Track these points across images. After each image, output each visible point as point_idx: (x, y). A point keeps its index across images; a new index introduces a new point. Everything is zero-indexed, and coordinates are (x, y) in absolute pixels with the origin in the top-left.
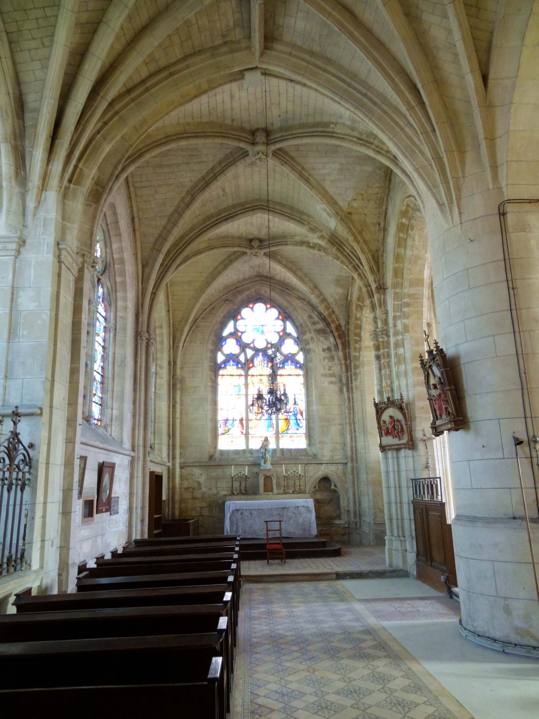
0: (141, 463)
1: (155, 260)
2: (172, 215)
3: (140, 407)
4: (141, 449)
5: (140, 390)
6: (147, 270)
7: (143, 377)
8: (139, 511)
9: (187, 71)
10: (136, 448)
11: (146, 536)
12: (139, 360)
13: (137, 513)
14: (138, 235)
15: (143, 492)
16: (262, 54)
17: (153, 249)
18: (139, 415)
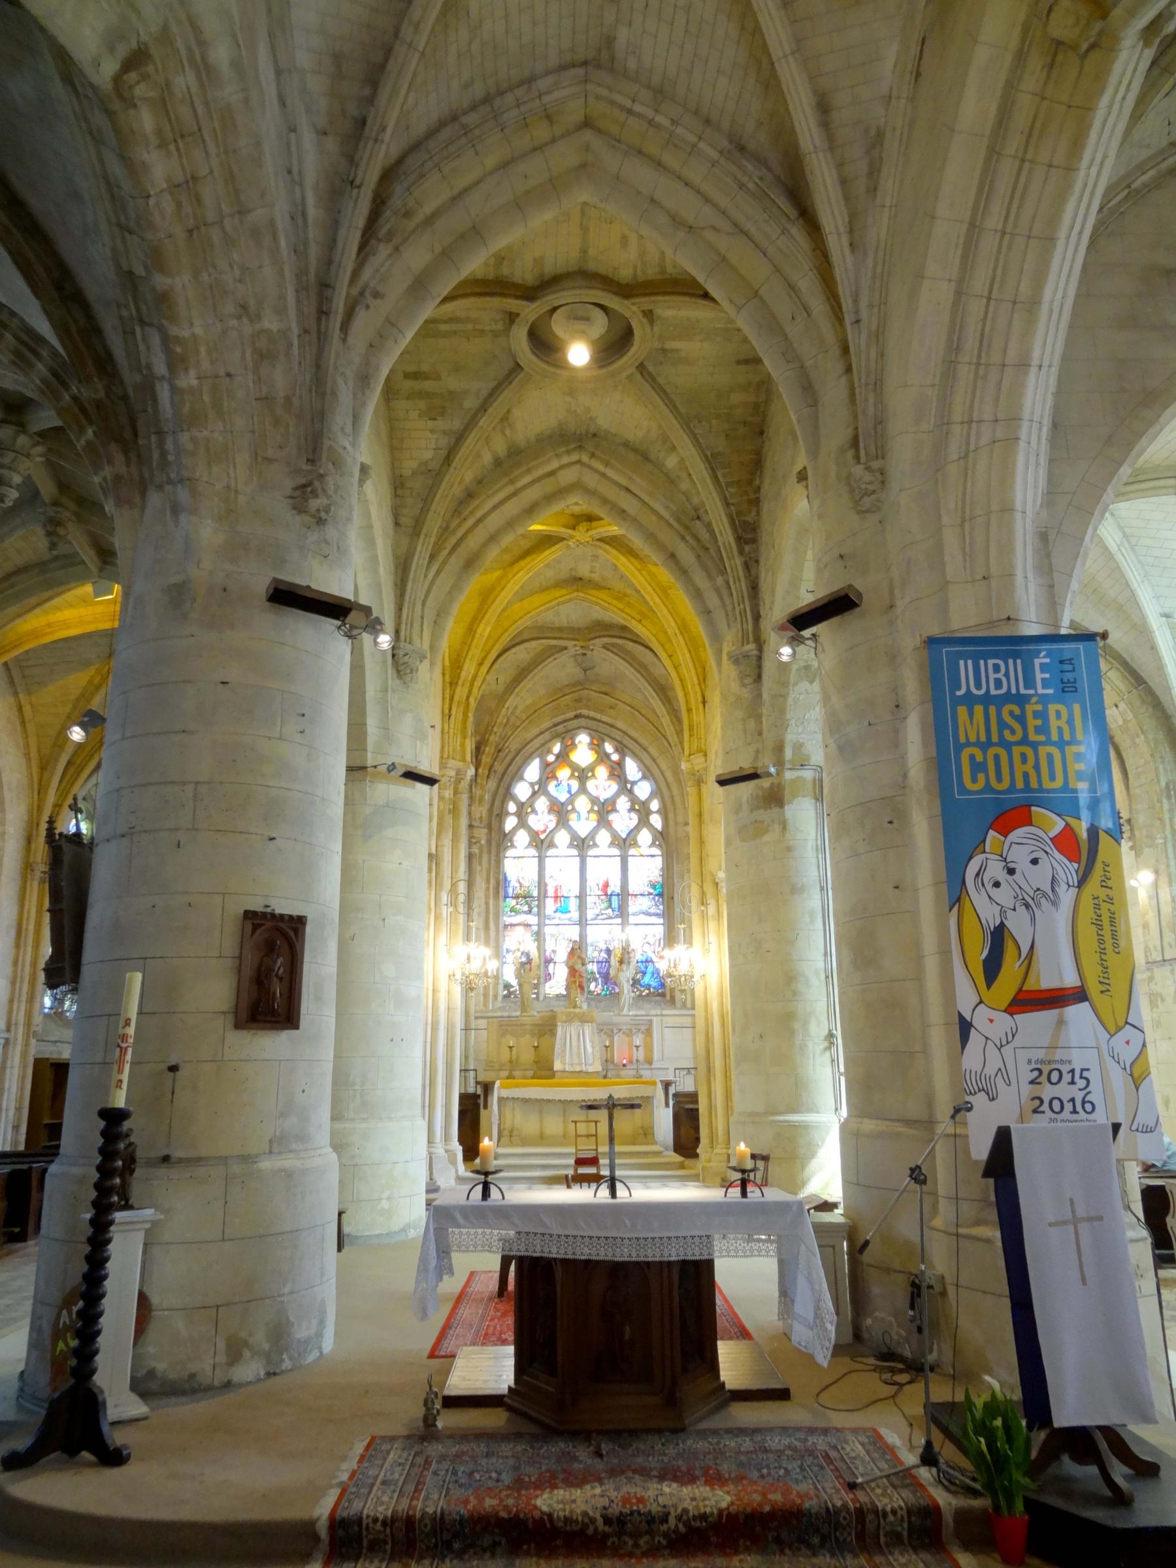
0: (19, 1048)
1: (57, 761)
2: (78, 699)
3: (22, 970)
4: (21, 1030)
5: (25, 946)
6: (46, 774)
7: (31, 927)
8: (12, 1113)
9: (10, 591)
10: (13, 1028)
11: (22, 1148)
12: (27, 903)
13: (7, 1116)
14: (30, 727)
15: (21, 1089)
16: (101, 570)
17: (54, 745)
18: (21, 982)
